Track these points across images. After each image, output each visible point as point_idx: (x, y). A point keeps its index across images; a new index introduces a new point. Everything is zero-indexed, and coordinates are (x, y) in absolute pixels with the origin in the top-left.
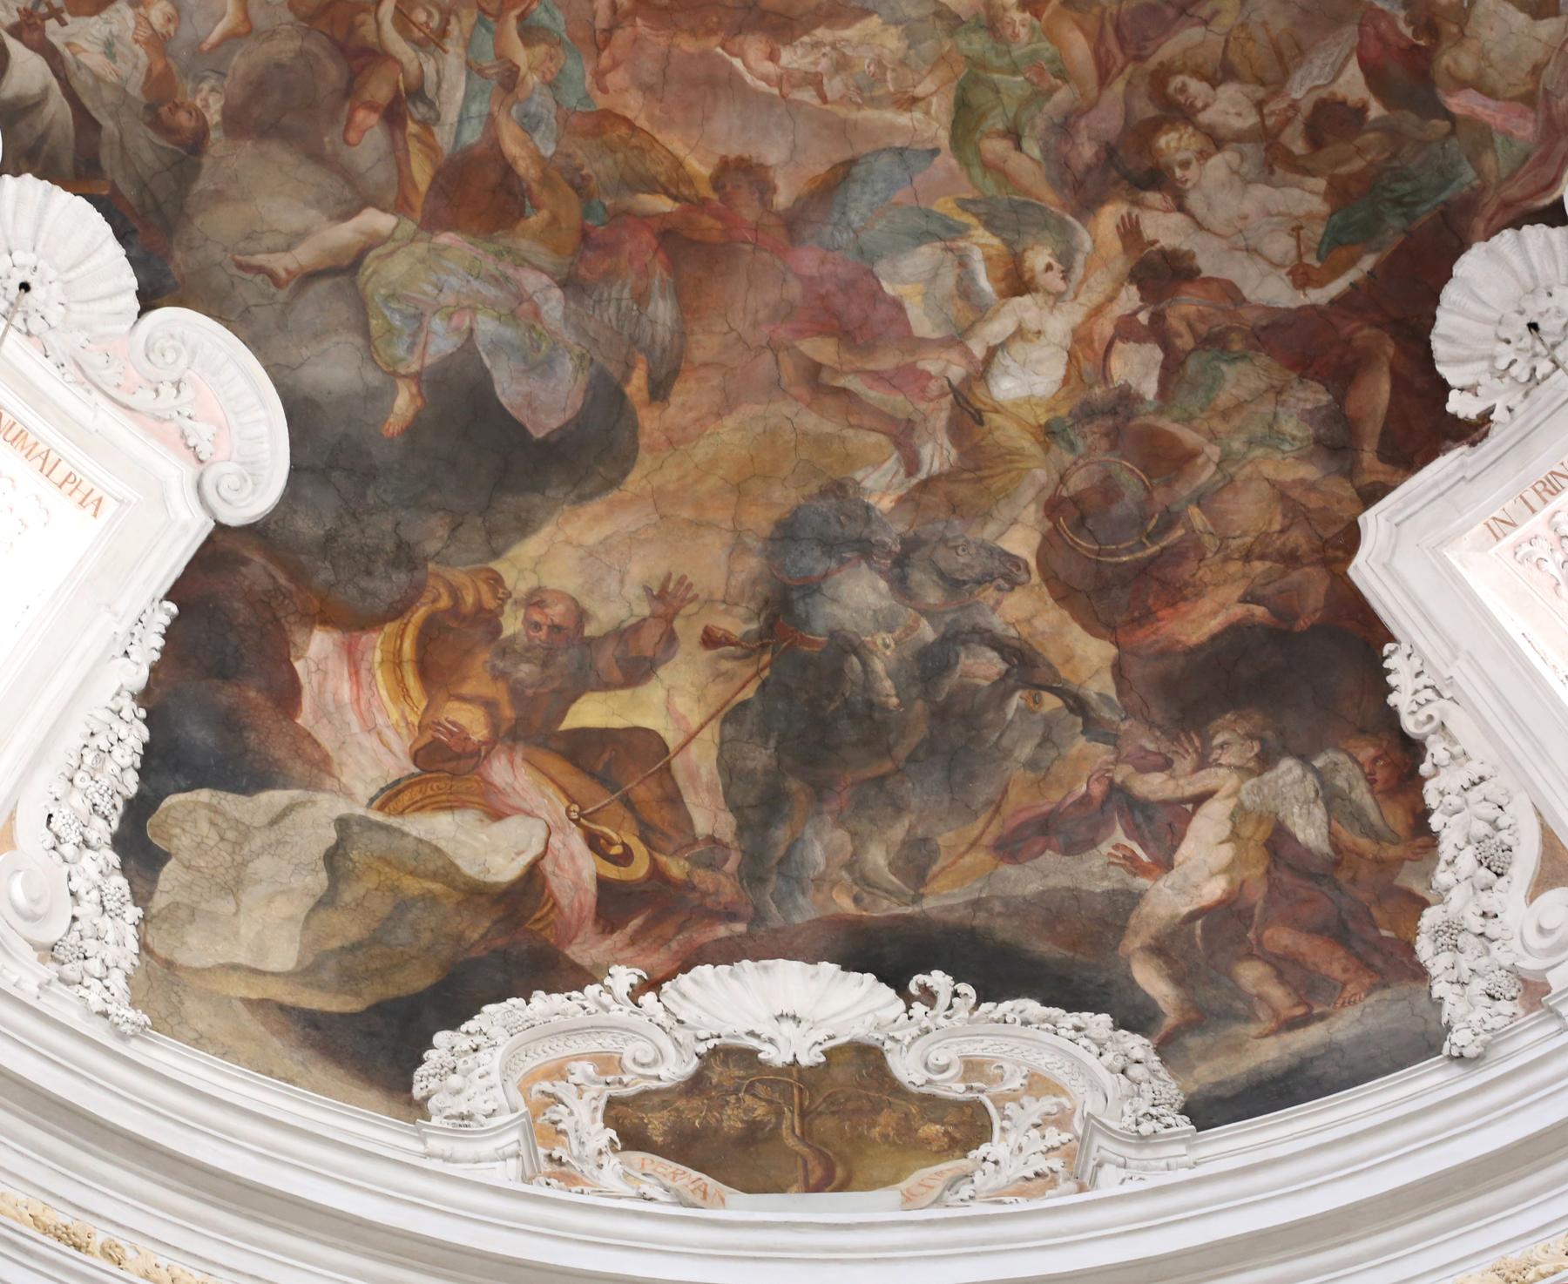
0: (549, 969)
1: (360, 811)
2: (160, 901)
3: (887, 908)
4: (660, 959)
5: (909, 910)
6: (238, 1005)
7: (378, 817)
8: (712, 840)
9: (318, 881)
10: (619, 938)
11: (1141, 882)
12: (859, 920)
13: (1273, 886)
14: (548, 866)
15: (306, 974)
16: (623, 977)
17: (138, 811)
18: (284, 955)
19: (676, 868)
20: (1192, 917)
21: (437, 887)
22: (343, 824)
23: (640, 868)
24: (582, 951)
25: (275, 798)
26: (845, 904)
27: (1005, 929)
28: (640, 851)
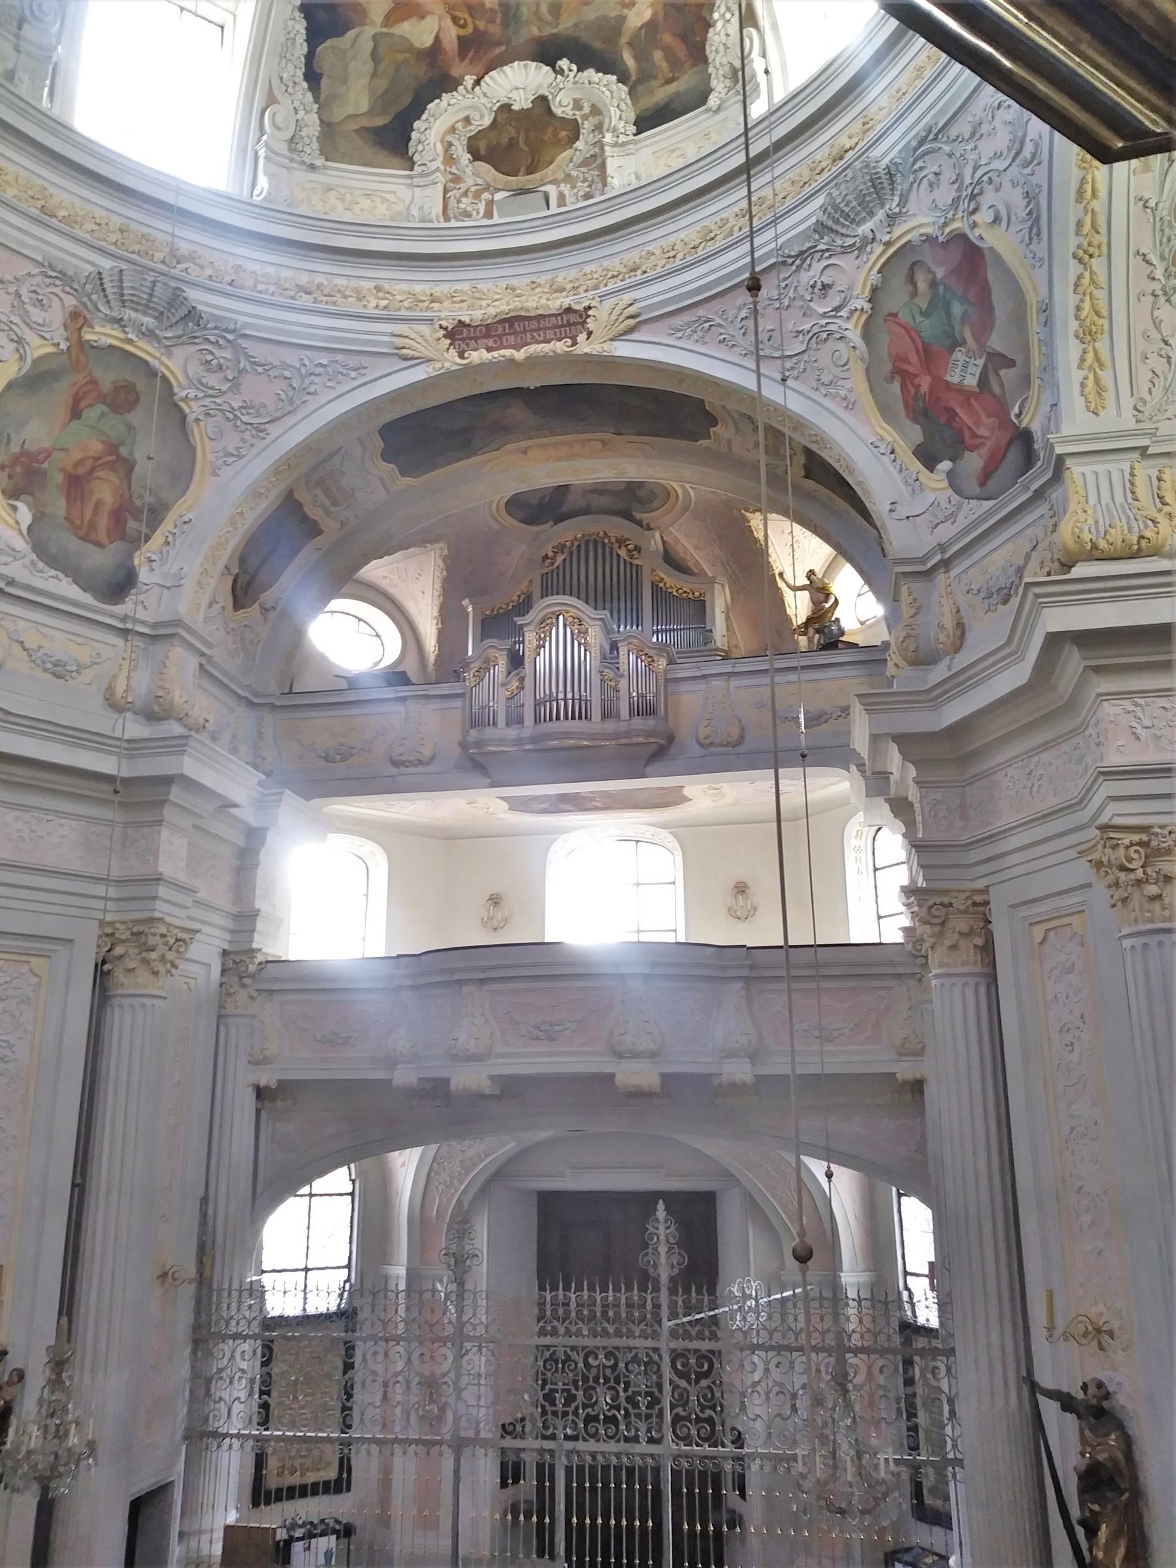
0: (444, 83)
1: (379, 30)
2: (323, 97)
3: (548, 31)
4: (479, 69)
5: (555, 31)
6: (353, 134)
7: (385, 30)
8: (492, 10)
9: (370, 66)
10: (466, 62)
11: (626, 11)
12: (540, 37)
13: (666, 14)
14: (441, 36)
15: (371, 112)
16: (469, 80)
17: (310, 57)
18: (364, 107)
19: (481, 25)
20: (641, 28)
21: (408, 55)
22: (374, 37)
23: (470, 30)
24: (455, 72)
25: (351, 34)
26: (535, 31)
27: (584, 37)
28: (469, 20)
